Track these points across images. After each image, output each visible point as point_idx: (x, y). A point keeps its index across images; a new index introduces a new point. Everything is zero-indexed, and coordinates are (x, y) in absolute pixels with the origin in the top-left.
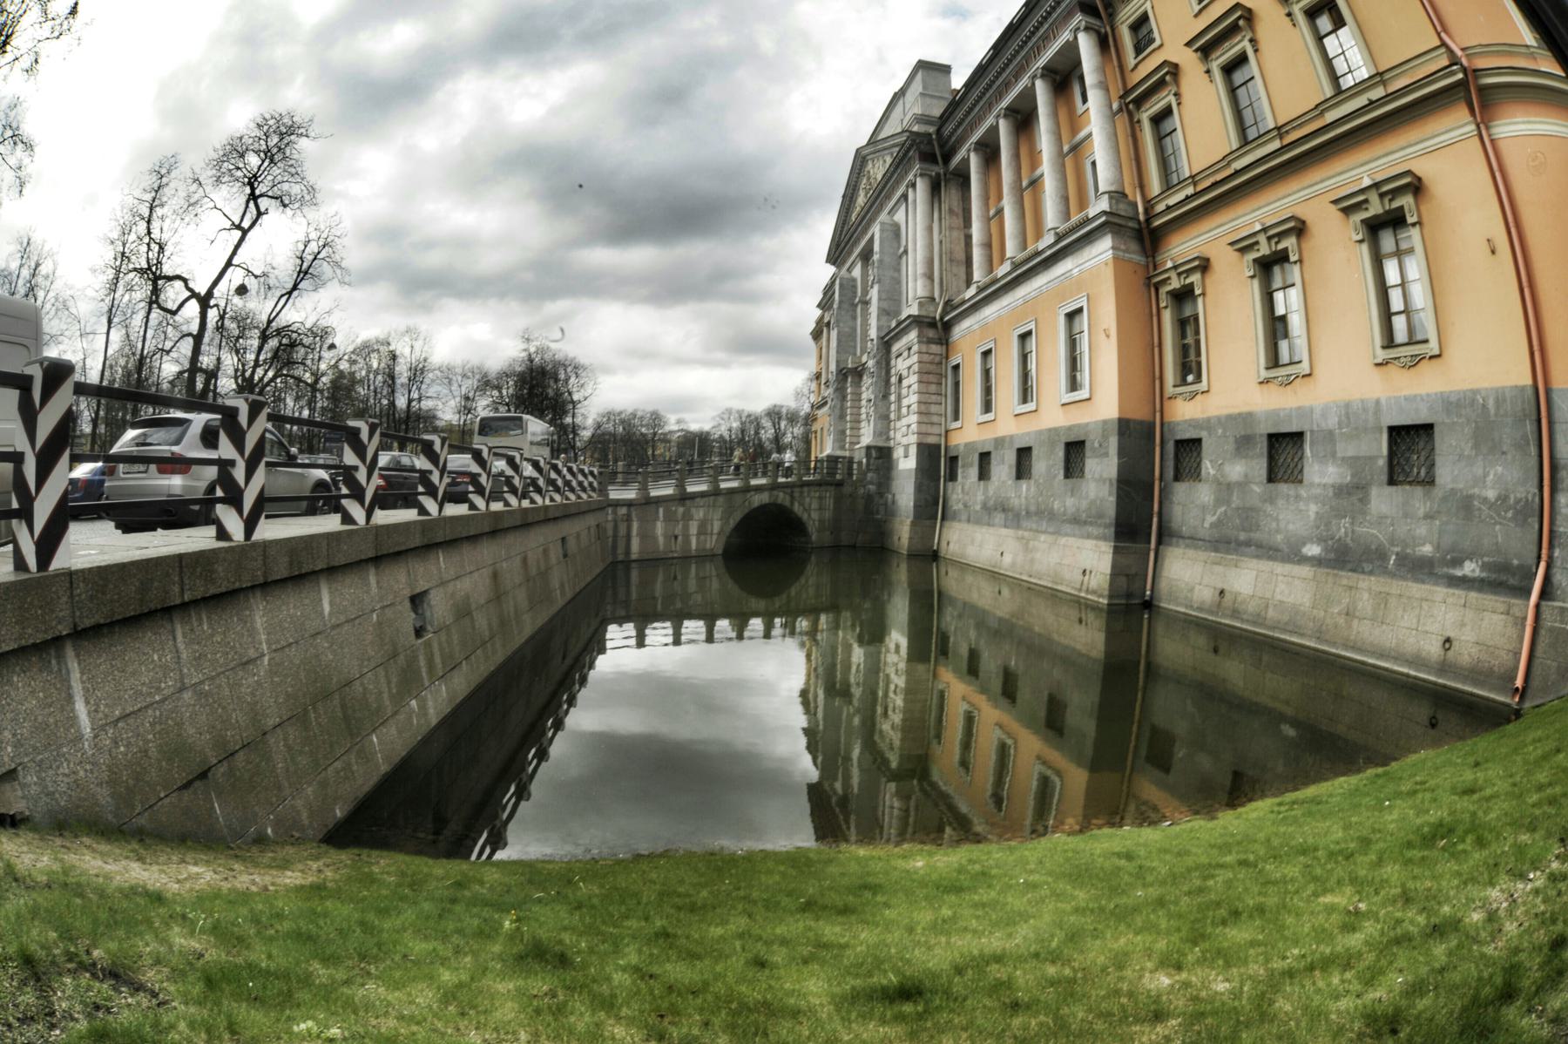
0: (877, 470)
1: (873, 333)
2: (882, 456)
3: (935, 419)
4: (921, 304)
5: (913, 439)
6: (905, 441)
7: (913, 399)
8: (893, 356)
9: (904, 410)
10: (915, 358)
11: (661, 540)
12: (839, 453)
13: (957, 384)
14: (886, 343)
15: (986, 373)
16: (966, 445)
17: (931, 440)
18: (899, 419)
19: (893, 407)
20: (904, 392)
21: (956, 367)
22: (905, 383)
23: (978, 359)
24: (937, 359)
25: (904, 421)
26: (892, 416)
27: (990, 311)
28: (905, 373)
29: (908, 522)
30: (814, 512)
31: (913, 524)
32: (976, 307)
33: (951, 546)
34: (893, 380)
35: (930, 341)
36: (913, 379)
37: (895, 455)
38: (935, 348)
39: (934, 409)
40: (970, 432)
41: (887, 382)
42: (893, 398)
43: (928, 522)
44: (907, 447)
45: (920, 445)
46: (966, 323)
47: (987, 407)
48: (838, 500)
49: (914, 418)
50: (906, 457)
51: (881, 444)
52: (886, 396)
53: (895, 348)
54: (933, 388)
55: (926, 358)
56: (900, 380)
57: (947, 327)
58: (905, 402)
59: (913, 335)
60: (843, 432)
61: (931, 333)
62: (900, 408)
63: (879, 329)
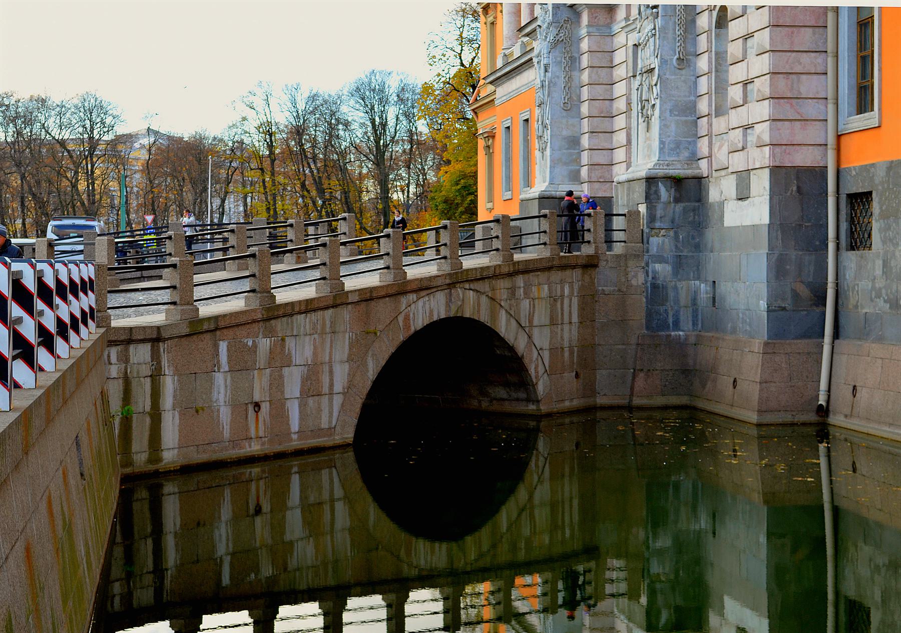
0: (674, 226)
5: (762, 157)
11: (225, 414)
18: (720, 111)
19: (703, 85)
26: (703, 106)
29: (757, 345)
30: (538, 328)
31: (769, 349)
33: (862, 394)
37: (713, 195)
42: (703, 64)
43: (803, 344)
44: (743, 178)
45: (777, 172)
48: (589, 300)
50: (743, 196)
51: (678, 171)
52: (686, 60)
62: (721, 87)
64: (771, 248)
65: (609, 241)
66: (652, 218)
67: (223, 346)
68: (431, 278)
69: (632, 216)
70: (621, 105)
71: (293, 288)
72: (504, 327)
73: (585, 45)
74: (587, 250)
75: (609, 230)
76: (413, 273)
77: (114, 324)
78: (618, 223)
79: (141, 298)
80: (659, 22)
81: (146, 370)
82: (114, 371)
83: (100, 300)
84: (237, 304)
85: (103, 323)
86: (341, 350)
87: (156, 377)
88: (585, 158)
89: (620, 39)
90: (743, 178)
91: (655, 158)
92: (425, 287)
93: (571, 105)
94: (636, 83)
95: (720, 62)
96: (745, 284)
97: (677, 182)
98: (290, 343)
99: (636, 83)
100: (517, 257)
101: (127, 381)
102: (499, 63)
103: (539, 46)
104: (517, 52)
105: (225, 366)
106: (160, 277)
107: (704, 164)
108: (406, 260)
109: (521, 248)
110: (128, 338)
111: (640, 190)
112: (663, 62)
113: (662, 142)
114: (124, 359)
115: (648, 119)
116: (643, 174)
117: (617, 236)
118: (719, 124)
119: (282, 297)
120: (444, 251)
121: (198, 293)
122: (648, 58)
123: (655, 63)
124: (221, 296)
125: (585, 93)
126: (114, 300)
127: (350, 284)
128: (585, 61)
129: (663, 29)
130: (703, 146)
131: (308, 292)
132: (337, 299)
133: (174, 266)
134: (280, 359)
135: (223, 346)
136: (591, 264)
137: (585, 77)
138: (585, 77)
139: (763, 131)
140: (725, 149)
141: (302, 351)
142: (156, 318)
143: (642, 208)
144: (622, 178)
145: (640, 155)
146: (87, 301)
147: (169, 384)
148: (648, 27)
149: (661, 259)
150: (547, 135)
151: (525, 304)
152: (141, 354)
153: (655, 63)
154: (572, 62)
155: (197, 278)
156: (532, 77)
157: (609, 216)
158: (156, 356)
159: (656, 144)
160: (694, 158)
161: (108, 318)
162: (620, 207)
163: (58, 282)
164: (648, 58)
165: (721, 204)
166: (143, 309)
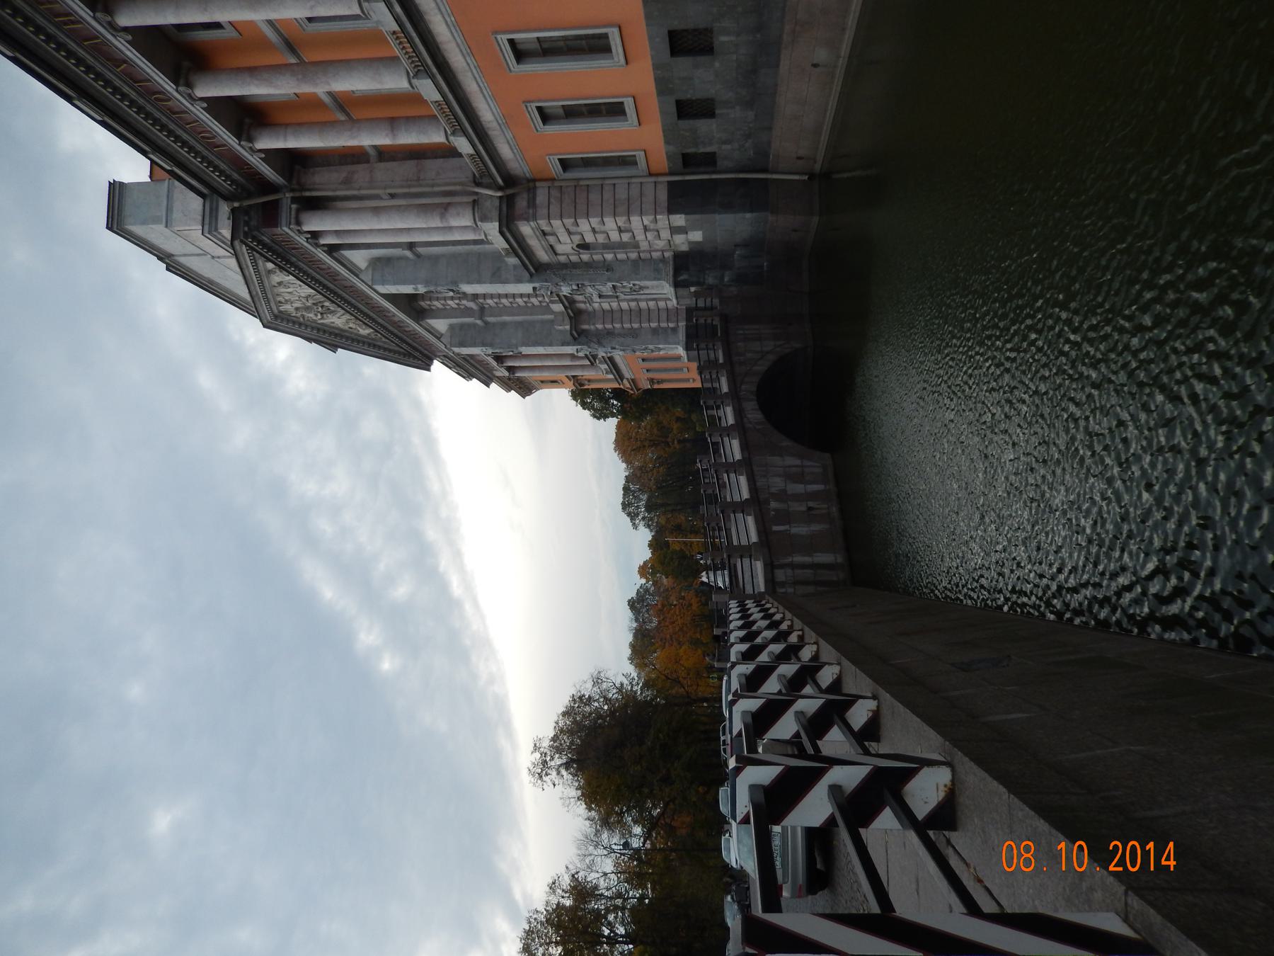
1: (526, 288)
2: (685, 266)
3: (635, 191)
4: (484, 218)
6: (665, 234)
7: (610, 224)
8: (554, 259)
9: (626, 237)
10: (557, 223)
12: (682, 335)
13: (587, 163)
14: (536, 269)
15: (572, 113)
16: (667, 142)
17: (663, 195)
18: (636, 246)
19: (621, 256)
20: (601, 239)
21: (565, 164)
22: (589, 238)
23: (552, 129)
24: (555, 193)
25: (640, 237)
26: (633, 256)
27: (487, 113)
28: (577, 239)
32: (481, 135)
34: (585, 257)
35: (532, 203)
36: (584, 226)
37: (685, 248)
38: (541, 197)
39: (622, 193)
40: (644, 136)
41: (589, 265)
42: (609, 257)
46: (505, 151)
47: (615, 111)
49: (636, 221)
51: (670, 269)
52: (608, 267)
53: (543, 256)
54: (595, 197)
55: (555, 208)
56: (584, 246)
57: (510, 181)
58: (615, 236)
59: (526, 229)
60: (655, 331)
61: (521, 203)
62: (621, 246)
63: (519, 281)
64: (714, 212)
65: (712, 308)
66: (697, 284)
67: (775, 528)
68: (734, 410)
69: (696, 295)
70: (633, 304)
71: (741, 488)
72: (762, 367)
73: (600, 326)
74: (717, 322)
75: (705, 309)
76: (731, 421)
77: (763, 589)
78: (701, 304)
79: (748, 574)
80: (586, 283)
81: (789, 571)
82: (790, 590)
83: (750, 597)
84: (750, 520)
85: (761, 595)
86: (777, 460)
87: (793, 566)
88: (664, 325)
89: (596, 306)
90: (675, 230)
91: (664, 283)
92: (739, 413)
93: (634, 334)
94: (622, 296)
95: (609, 246)
96: (732, 226)
97: (677, 272)
98: (773, 490)
99: (622, 296)
100: (721, 361)
101: (796, 583)
102: (611, 376)
103: (601, 353)
104: (604, 366)
105: (787, 527)
106: (735, 566)
107: (667, 255)
108: (724, 424)
109: (717, 360)
110: (770, 581)
111: (682, 291)
112: (610, 280)
113: (655, 279)
114: (783, 584)
115: (641, 288)
116: (672, 289)
117: (708, 304)
118: (644, 245)
119: (746, 495)
120: (719, 402)
121: (744, 542)
122: (607, 289)
123: (610, 284)
124: (747, 530)
125: (627, 326)
126: (749, 590)
127: (738, 456)
128: (609, 326)
129: (591, 281)
130: (656, 255)
131: (743, 480)
132: (746, 465)
133: (729, 557)
134: (782, 496)
135: (775, 528)
136: (725, 319)
137: (618, 326)
138: (618, 326)
139: (647, 220)
140: (658, 242)
141: (777, 483)
142: (759, 566)
143: (693, 289)
144: (675, 301)
145: (663, 291)
146: (750, 604)
147: (798, 559)
148: (589, 290)
149: (722, 278)
150: (651, 347)
151: (749, 355)
152: (780, 575)
153: (610, 284)
154: (610, 333)
155: (735, 543)
156: (618, 356)
157: (697, 309)
158: (782, 566)
159: (655, 283)
160: (663, 260)
161: (760, 593)
162: (690, 302)
163: (740, 619)
164: (607, 289)
165: (690, 243)
166: (755, 574)
